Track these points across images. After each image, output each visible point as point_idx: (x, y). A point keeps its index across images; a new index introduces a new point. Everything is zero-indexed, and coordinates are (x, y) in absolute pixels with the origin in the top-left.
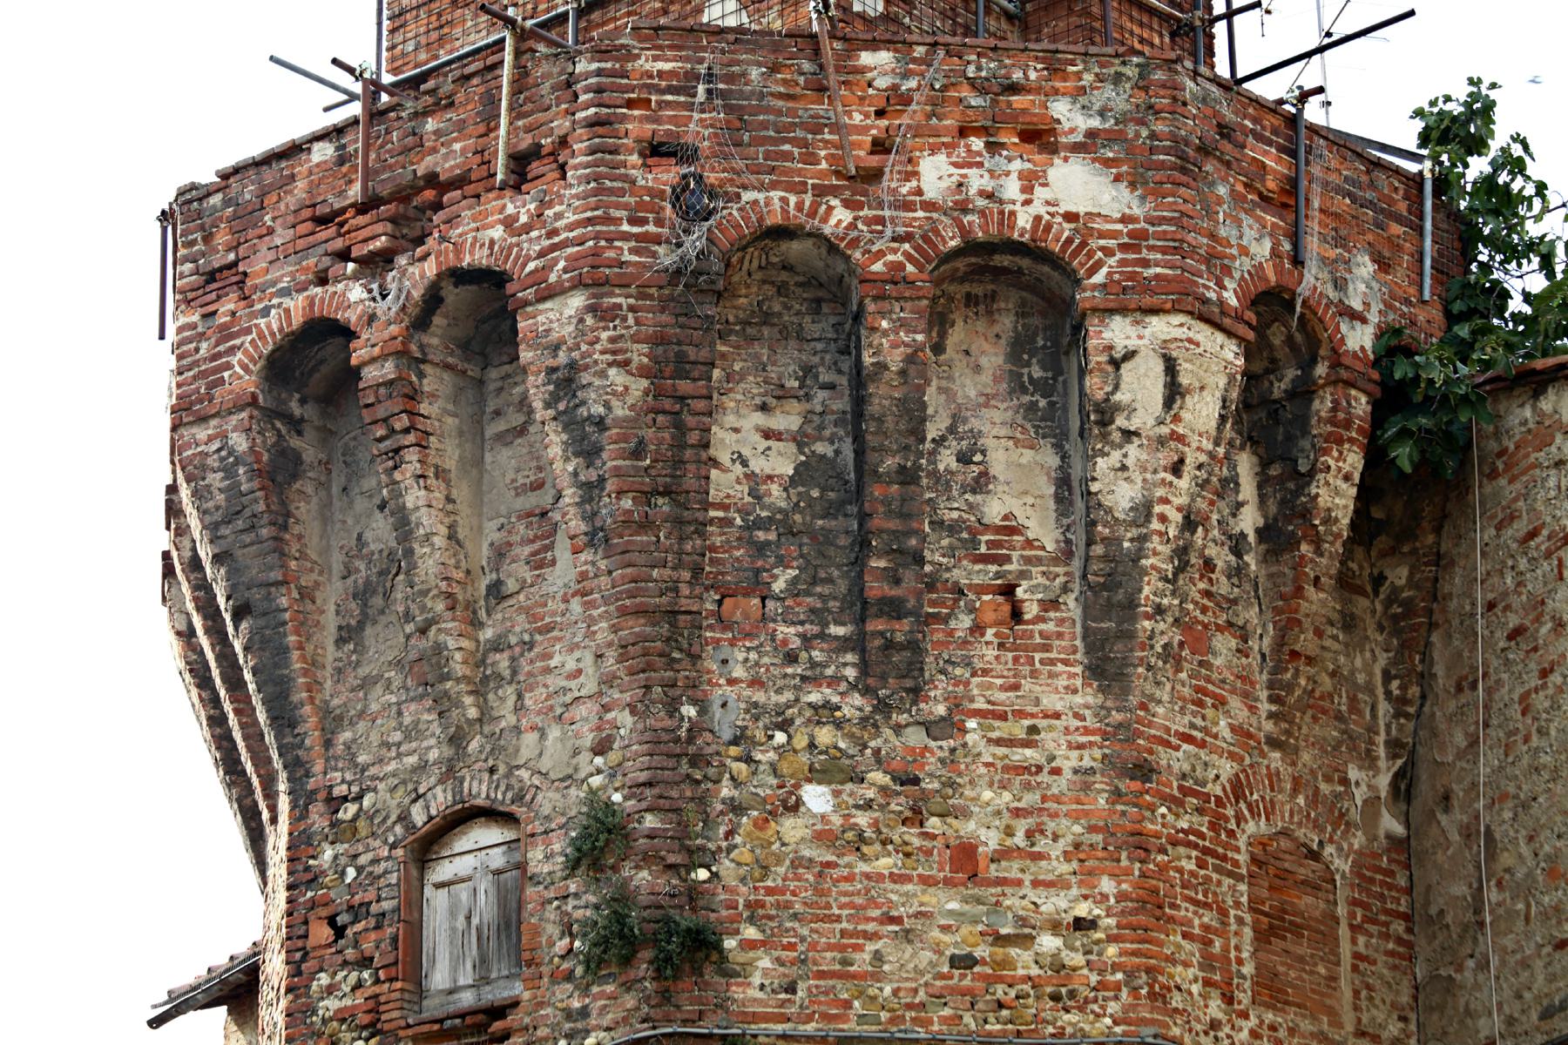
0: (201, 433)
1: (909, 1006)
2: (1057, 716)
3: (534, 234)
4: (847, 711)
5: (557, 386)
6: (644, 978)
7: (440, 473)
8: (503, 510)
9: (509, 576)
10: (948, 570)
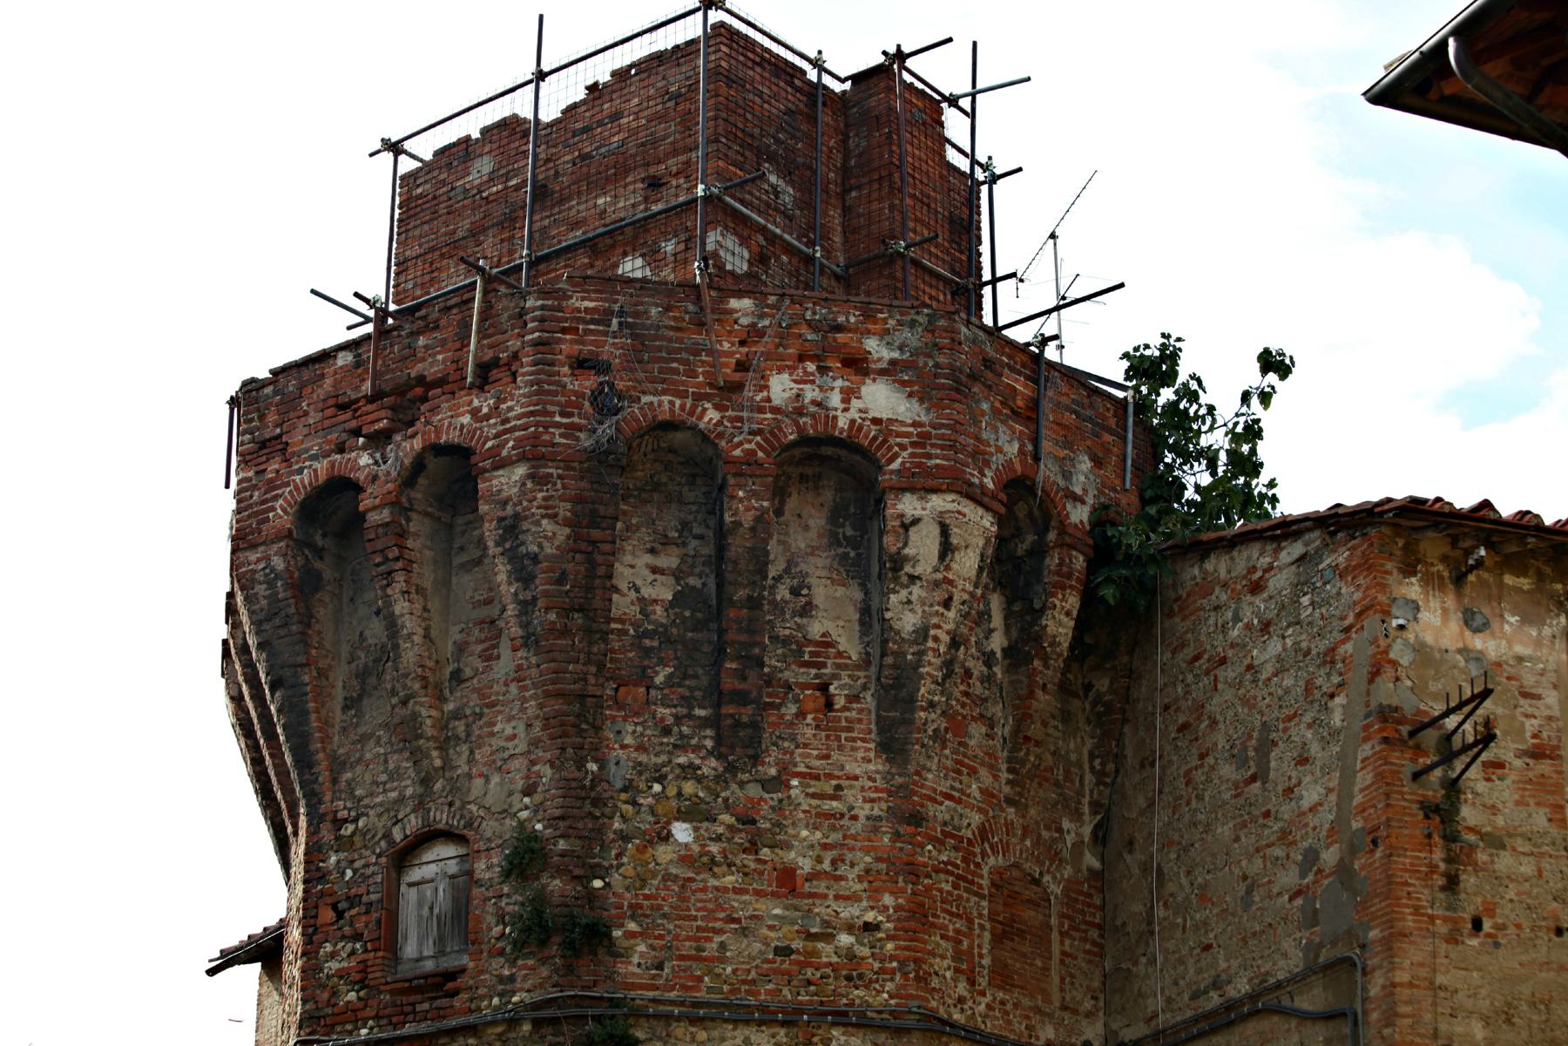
0: (253, 557)
1: (744, 982)
2: (856, 778)
4: (705, 770)
7: (420, 590)
10: (781, 671)
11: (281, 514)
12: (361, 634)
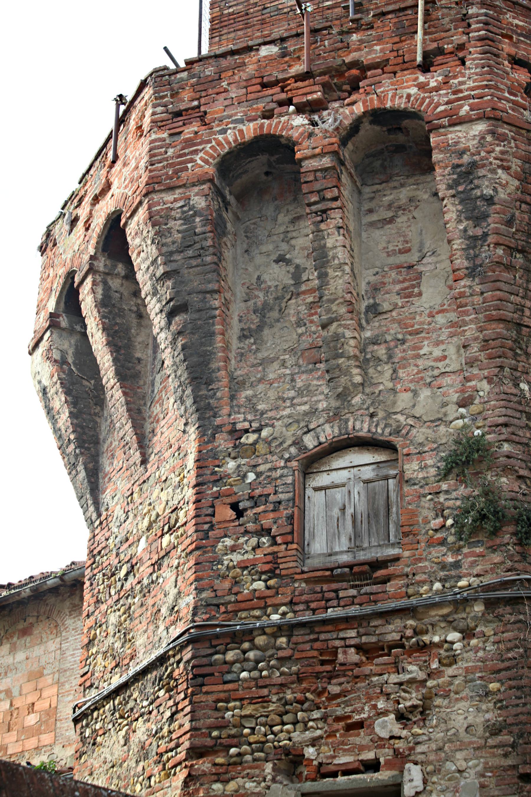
0: (169, 197)
3: (441, 92)
5: (460, 175)
6: (508, 544)
8: (378, 263)
9: (384, 301)
11: (202, 162)
12: (259, 278)
